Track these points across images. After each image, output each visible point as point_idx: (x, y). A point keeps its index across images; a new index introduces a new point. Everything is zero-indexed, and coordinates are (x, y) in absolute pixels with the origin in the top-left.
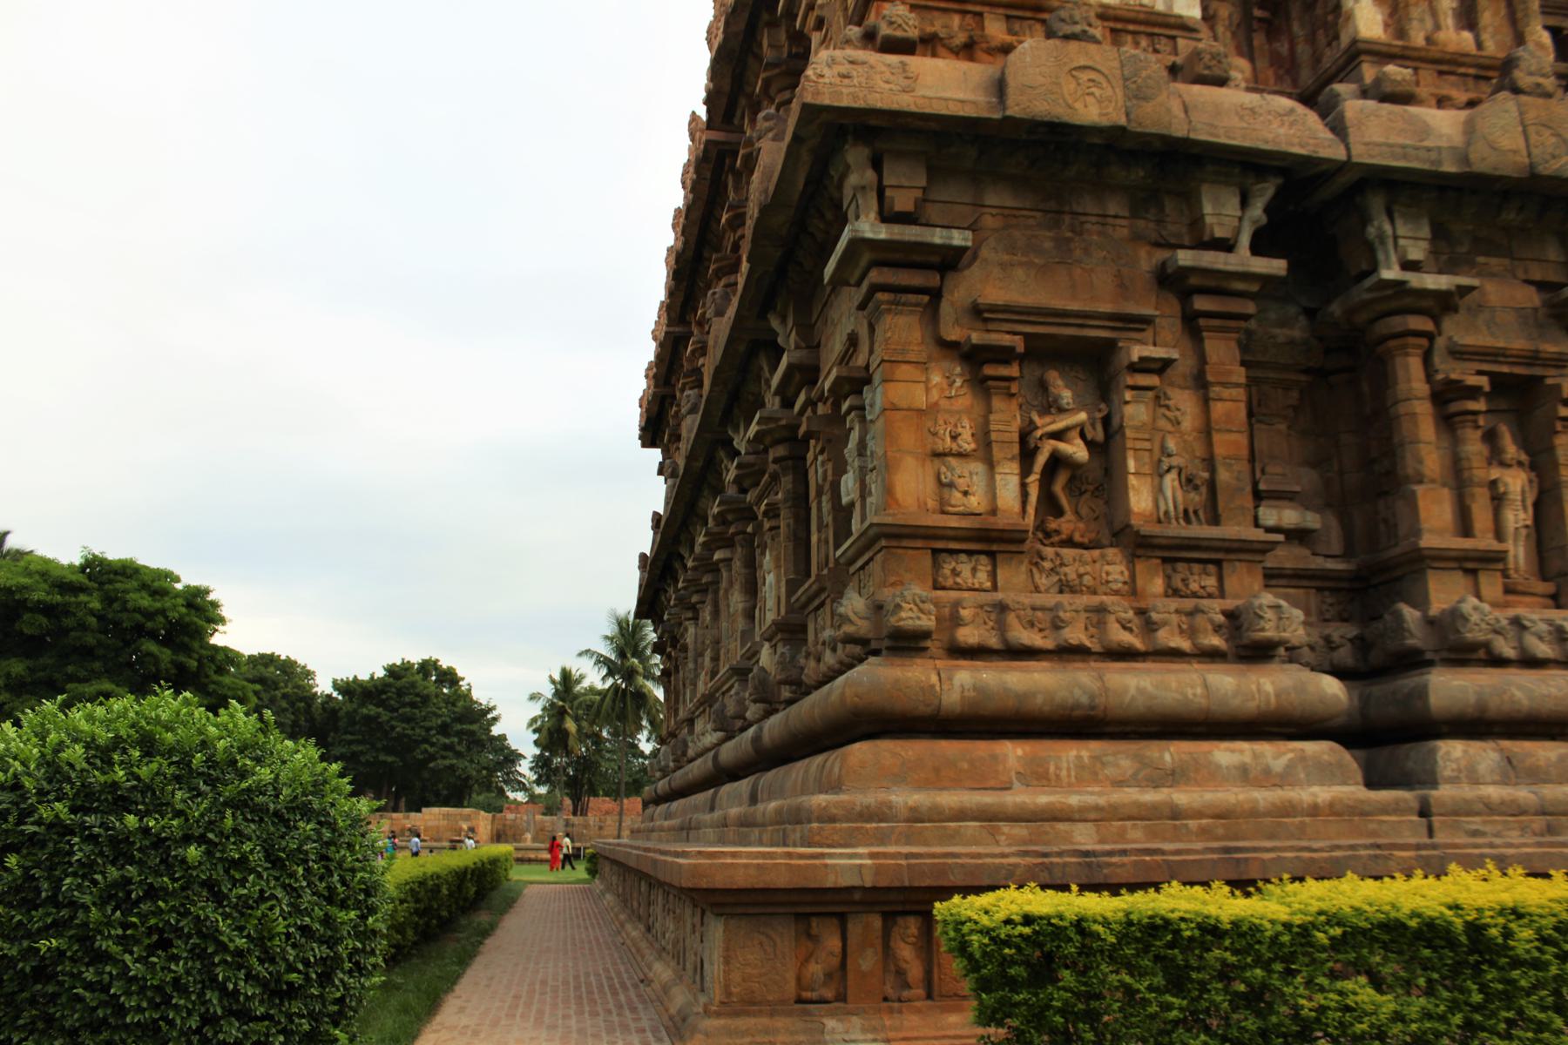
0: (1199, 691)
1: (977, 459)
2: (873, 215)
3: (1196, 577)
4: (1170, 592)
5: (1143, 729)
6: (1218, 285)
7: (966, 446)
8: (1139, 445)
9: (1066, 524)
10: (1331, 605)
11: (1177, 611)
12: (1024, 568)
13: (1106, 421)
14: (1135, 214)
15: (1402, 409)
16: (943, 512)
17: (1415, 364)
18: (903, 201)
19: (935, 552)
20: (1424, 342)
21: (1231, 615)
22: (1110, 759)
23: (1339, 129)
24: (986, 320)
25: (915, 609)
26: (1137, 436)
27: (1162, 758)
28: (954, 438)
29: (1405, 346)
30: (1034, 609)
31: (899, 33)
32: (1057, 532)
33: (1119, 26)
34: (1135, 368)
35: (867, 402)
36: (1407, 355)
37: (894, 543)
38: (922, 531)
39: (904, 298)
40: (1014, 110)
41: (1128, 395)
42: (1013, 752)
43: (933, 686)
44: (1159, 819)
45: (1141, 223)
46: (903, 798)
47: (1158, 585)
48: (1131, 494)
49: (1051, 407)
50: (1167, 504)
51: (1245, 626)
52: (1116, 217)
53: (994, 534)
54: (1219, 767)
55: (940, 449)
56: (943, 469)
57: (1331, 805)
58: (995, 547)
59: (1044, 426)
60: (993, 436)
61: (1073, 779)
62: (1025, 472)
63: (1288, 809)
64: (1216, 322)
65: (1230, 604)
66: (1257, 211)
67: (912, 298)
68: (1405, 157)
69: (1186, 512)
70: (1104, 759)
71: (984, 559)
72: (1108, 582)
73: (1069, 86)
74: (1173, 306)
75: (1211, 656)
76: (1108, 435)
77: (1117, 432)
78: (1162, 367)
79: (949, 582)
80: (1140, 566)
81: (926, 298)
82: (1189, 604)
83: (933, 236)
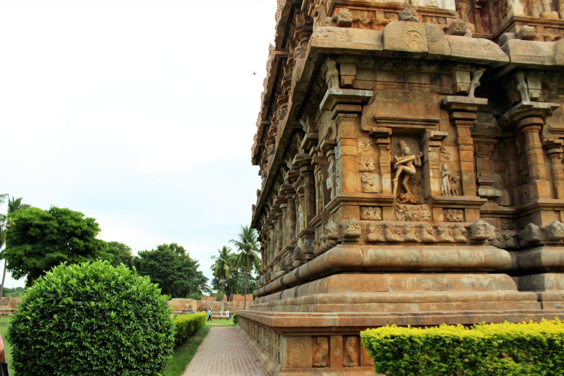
0: (456, 256)
1: (376, 173)
2: (337, 86)
3: (455, 215)
4: (446, 220)
5: (436, 270)
6: (462, 108)
8: (434, 167)
9: (408, 196)
10: (506, 224)
11: (448, 227)
12: (392, 212)
13: (422, 158)
14: (432, 83)
15: (531, 152)
16: (363, 192)
17: (536, 135)
18: (347, 81)
19: (361, 206)
20: (539, 127)
21: (468, 228)
22: (424, 280)
23: (506, 50)
24: (378, 123)
25: (354, 227)
27: (443, 280)
28: (367, 165)
29: (532, 129)
30: (396, 227)
31: (345, 20)
32: (405, 199)
33: (425, 14)
34: (432, 139)
35: (336, 153)
36: (533, 132)
37: (346, 204)
39: (349, 115)
40: (387, 47)
41: (430, 149)
42: (389, 278)
43: (360, 255)
44: (442, 302)
45: (434, 86)
46: (350, 295)
47: (441, 217)
48: (431, 185)
49: (402, 153)
50: (444, 188)
51: (473, 232)
52: (425, 84)
53: (382, 200)
54: (464, 283)
55: (362, 169)
56: (363, 177)
57: (505, 297)
58: (382, 205)
59: (399, 160)
60: (381, 165)
61: (411, 288)
62: (393, 177)
63: (489, 299)
65: (467, 224)
66: (476, 81)
67: (351, 115)
68: (531, 60)
69: (451, 191)
70: (422, 281)
71: (378, 209)
72: (423, 217)
73: (407, 38)
74: (446, 116)
75: (461, 243)
76: (423, 164)
77: (426, 162)
78: (442, 139)
79: (366, 217)
80: (435, 211)
81: (356, 115)
82: (453, 224)
83: (359, 93)
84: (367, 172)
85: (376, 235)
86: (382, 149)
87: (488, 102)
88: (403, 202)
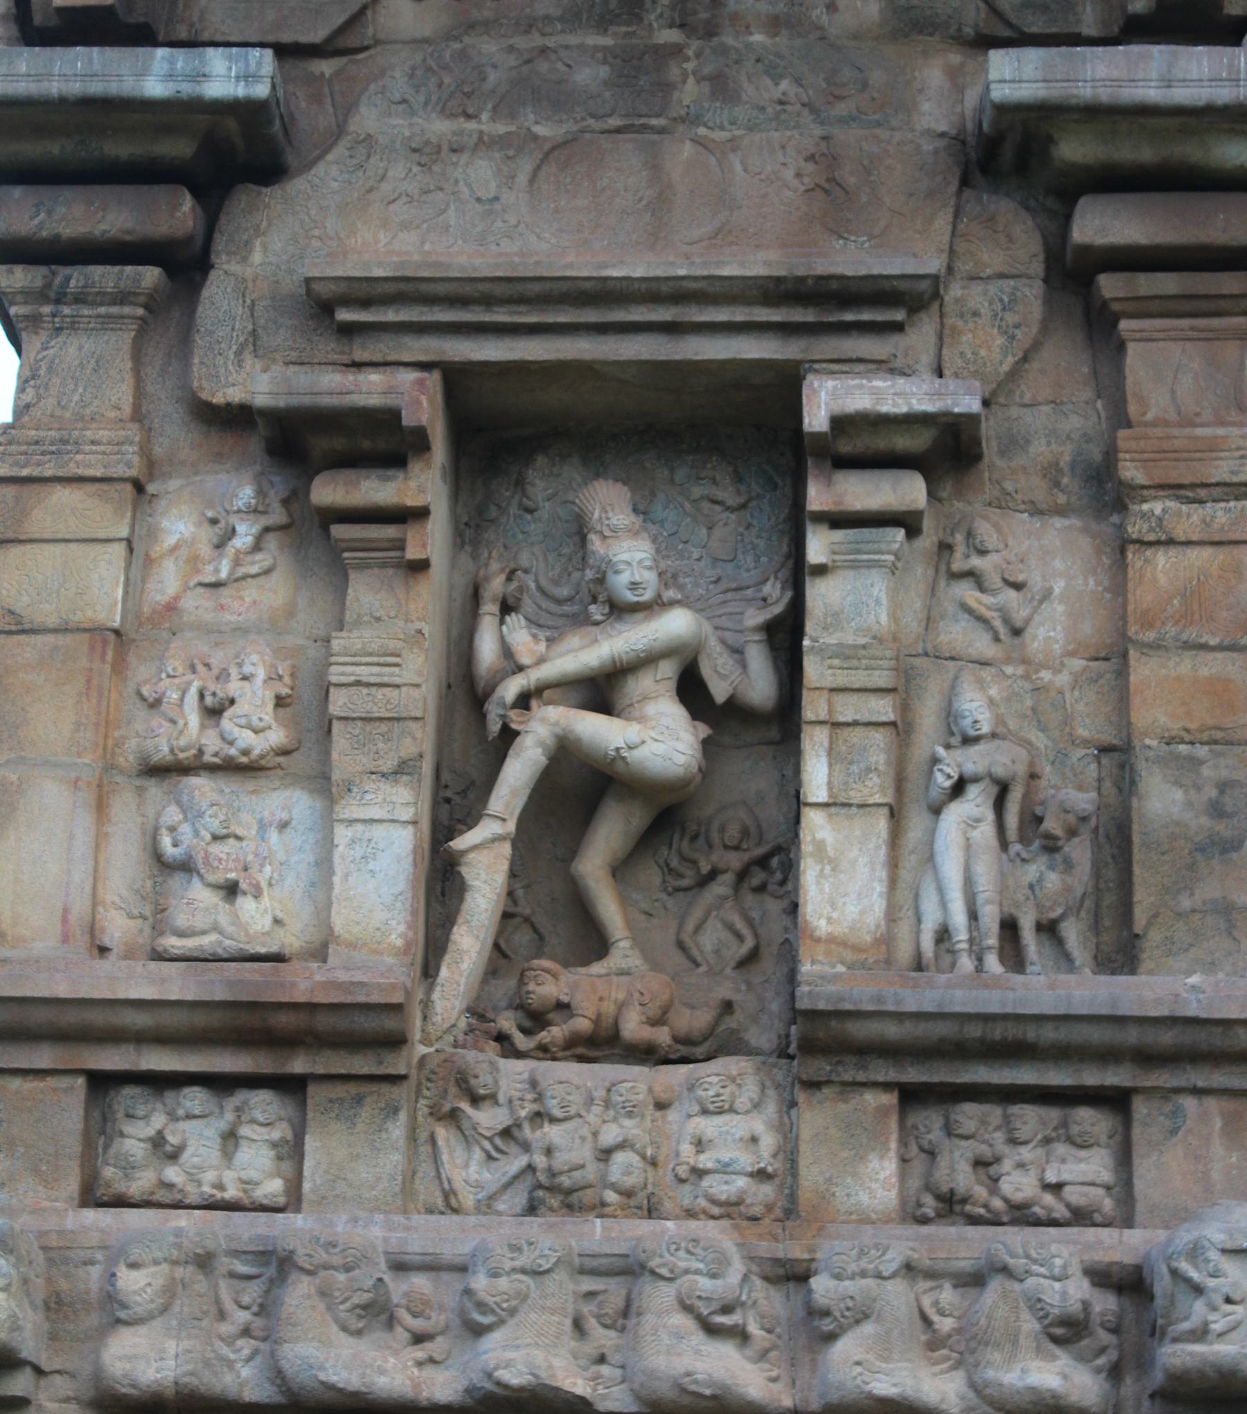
3: (1025, 1153)
4: (930, 1205)
7: (246, 738)
8: (848, 709)
11: (910, 1269)
12: (397, 1130)
16: (159, 956)
24: (349, 331)
26: (843, 679)
28: (213, 712)
30: (400, 1266)
38: (40, 1016)
39: (76, 277)
50: (943, 904)
53: (283, 1020)
55: (162, 750)
56: (172, 814)
58: (298, 1065)
60: (339, 703)
64: (1167, 283)
67: (104, 276)
69: (1009, 927)
72: (699, 1173)
81: (151, 275)
83: (142, 74)
84: (212, 769)
85: (171, 1346)
86: (363, 566)
88: (544, 1036)
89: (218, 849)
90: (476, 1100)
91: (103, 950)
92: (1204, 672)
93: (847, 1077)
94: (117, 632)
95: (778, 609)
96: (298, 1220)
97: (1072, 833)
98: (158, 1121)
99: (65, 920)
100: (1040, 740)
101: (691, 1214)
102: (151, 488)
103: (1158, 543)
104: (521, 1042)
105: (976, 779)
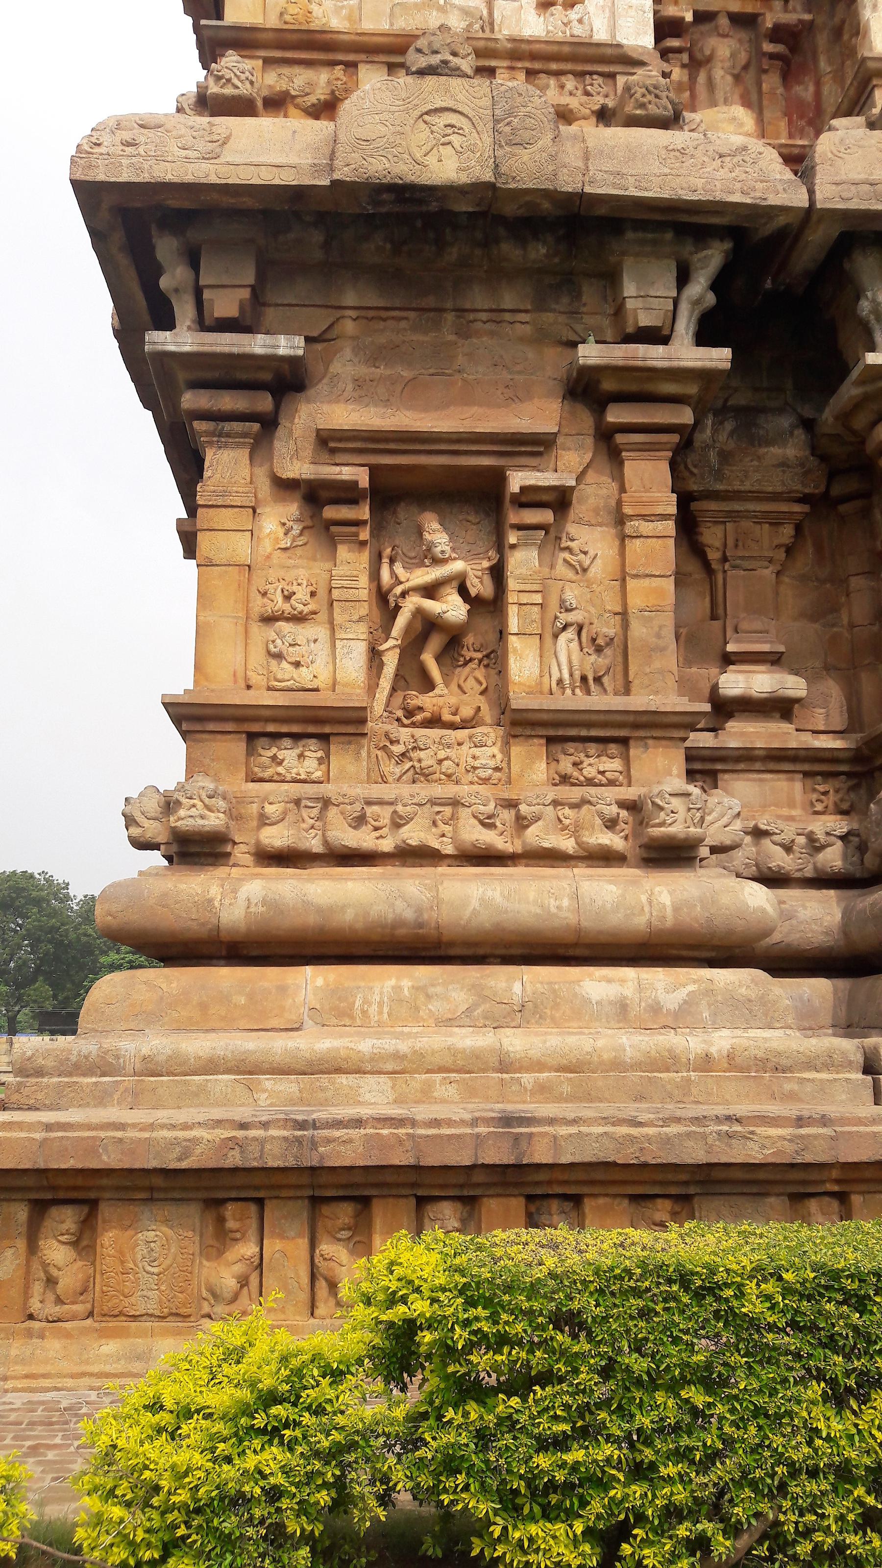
0: (566, 903)
3: (592, 760)
7: (300, 607)
11: (556, 803)
21: (632, 807)
22: (439, 989)
24: (333, 451)
25: (199, 804)
30: (369, 803)
31: (228, 91)
32: (420, 709)
33: (537, 66)
37: (198, 727)
39: (228, 426)
43: (210, 901)
44: (484, 1071)
45: (548, 318)
54: (587, 1001)
57: (730, 1057)
58: (327, 730)
60: (336, 594)
65: (630, 793)
69: (584, 679)
70: (431, 990)
72: (475, 768)
74: (586, 420)
80: (517, 750)
81: (256, 426)
84: (288, 619)
85: (286, 833)
86: (343, 542)
87: (733, 361)
89: (291, 649)
90: (392, 742)
91: (249, 687)
92: (654, 585)
93: (528, 733)
94: (249, 566)
95: (494, 562)
96: (329, 786)
97: (607, 644)
98: (274, 750)
99: (235, 675)
100: (593, 610)
101: (472, 783)
102: (258, 511)
103: (637, 537)
104: (406, 721)
105: (571, 625)
